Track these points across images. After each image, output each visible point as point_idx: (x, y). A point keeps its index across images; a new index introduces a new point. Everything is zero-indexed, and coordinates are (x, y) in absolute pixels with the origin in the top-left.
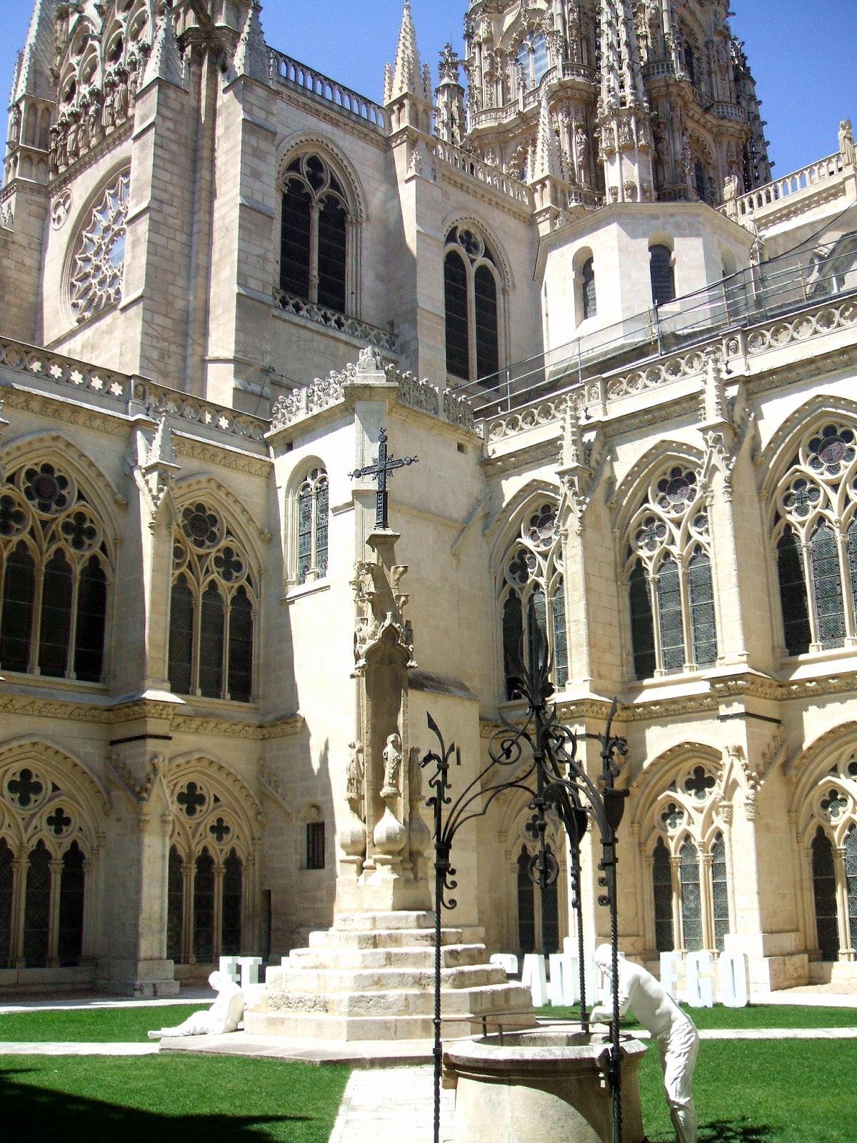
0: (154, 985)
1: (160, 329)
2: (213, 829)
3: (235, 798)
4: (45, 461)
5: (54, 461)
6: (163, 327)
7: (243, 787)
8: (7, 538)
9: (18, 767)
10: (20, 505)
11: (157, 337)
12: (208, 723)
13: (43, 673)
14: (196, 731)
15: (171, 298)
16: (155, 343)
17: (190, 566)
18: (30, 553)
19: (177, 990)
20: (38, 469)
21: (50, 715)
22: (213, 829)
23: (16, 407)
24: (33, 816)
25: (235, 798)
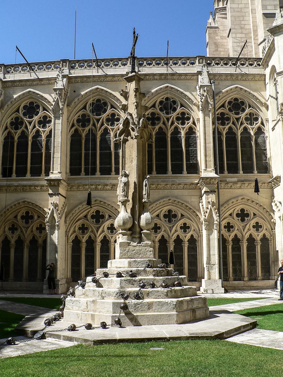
0: (212, 290)
1: (240, 39)
2: (254, 227)
3: (262, 214)
4: (166, 96)
5: (169, 96)
6: (241, 38)
7: (264, 208)
8: (153, 127)
9: (166, 208)
10: (158, 114)
11: (238, 42)
12: (244, 184)
13: (228, 173)
14: (240, 188)
15: (243, 26)
16: (238, 44)
17: (233, 123)
18: (164, 130)
19: (223, 291)
20: (164, 100)
21: (175, 188)
22: (254, 227)
23: (150, 80)
24: (173, 226)
25: (262, 214)
